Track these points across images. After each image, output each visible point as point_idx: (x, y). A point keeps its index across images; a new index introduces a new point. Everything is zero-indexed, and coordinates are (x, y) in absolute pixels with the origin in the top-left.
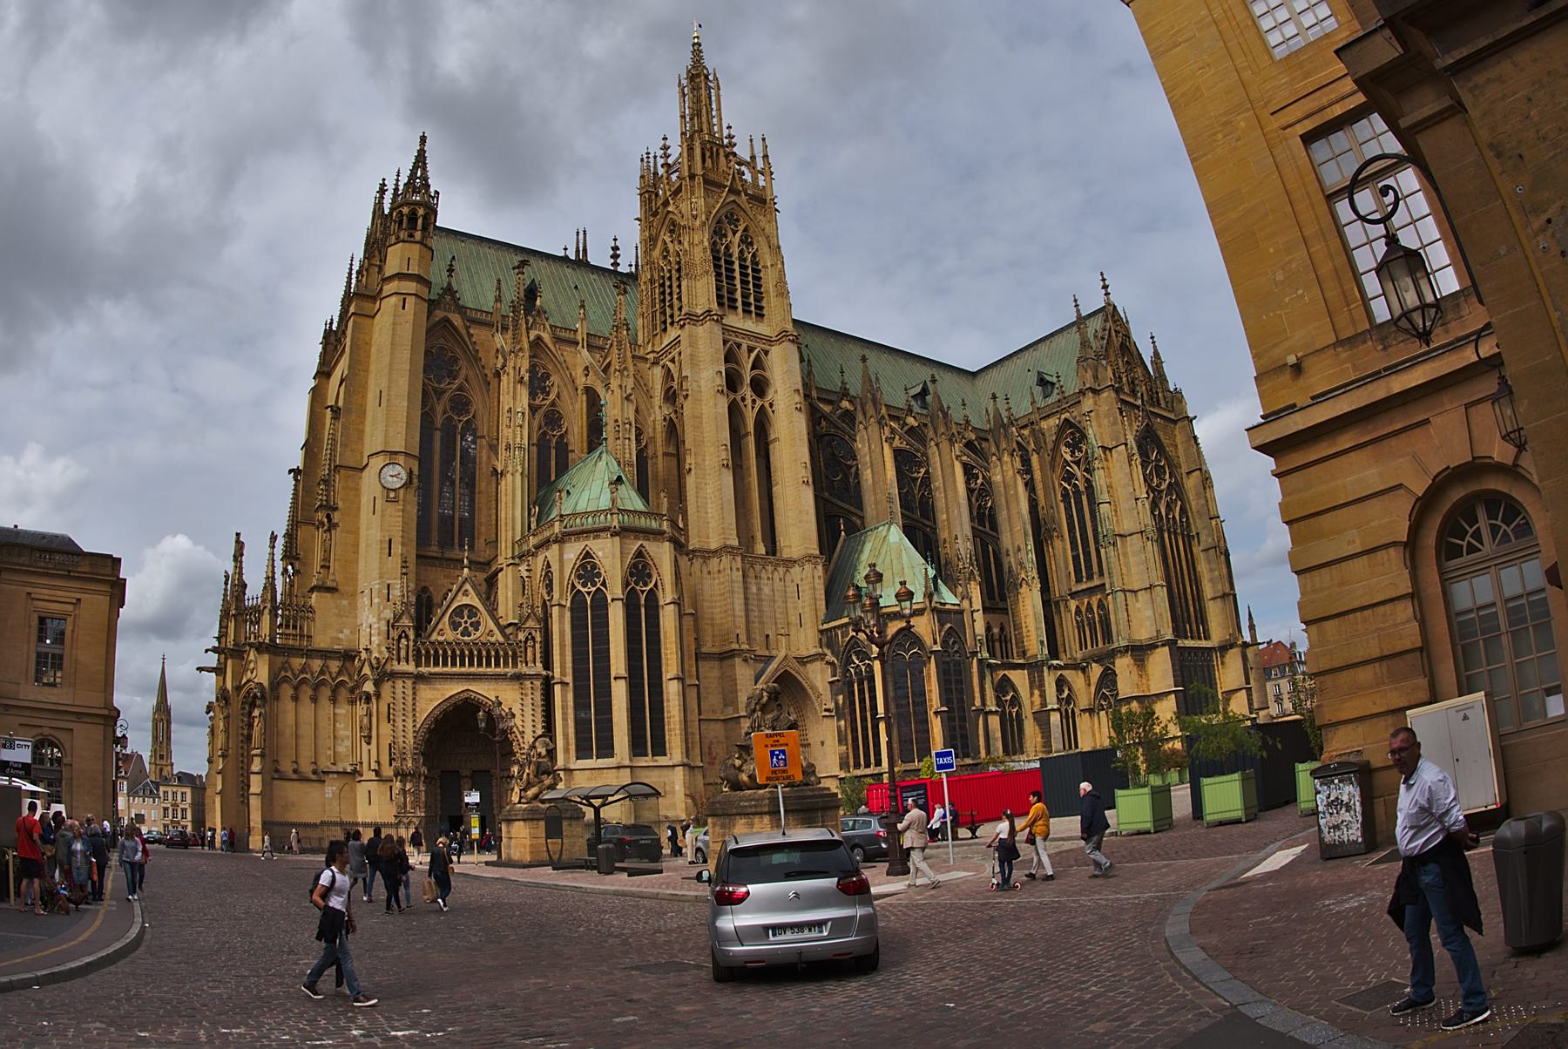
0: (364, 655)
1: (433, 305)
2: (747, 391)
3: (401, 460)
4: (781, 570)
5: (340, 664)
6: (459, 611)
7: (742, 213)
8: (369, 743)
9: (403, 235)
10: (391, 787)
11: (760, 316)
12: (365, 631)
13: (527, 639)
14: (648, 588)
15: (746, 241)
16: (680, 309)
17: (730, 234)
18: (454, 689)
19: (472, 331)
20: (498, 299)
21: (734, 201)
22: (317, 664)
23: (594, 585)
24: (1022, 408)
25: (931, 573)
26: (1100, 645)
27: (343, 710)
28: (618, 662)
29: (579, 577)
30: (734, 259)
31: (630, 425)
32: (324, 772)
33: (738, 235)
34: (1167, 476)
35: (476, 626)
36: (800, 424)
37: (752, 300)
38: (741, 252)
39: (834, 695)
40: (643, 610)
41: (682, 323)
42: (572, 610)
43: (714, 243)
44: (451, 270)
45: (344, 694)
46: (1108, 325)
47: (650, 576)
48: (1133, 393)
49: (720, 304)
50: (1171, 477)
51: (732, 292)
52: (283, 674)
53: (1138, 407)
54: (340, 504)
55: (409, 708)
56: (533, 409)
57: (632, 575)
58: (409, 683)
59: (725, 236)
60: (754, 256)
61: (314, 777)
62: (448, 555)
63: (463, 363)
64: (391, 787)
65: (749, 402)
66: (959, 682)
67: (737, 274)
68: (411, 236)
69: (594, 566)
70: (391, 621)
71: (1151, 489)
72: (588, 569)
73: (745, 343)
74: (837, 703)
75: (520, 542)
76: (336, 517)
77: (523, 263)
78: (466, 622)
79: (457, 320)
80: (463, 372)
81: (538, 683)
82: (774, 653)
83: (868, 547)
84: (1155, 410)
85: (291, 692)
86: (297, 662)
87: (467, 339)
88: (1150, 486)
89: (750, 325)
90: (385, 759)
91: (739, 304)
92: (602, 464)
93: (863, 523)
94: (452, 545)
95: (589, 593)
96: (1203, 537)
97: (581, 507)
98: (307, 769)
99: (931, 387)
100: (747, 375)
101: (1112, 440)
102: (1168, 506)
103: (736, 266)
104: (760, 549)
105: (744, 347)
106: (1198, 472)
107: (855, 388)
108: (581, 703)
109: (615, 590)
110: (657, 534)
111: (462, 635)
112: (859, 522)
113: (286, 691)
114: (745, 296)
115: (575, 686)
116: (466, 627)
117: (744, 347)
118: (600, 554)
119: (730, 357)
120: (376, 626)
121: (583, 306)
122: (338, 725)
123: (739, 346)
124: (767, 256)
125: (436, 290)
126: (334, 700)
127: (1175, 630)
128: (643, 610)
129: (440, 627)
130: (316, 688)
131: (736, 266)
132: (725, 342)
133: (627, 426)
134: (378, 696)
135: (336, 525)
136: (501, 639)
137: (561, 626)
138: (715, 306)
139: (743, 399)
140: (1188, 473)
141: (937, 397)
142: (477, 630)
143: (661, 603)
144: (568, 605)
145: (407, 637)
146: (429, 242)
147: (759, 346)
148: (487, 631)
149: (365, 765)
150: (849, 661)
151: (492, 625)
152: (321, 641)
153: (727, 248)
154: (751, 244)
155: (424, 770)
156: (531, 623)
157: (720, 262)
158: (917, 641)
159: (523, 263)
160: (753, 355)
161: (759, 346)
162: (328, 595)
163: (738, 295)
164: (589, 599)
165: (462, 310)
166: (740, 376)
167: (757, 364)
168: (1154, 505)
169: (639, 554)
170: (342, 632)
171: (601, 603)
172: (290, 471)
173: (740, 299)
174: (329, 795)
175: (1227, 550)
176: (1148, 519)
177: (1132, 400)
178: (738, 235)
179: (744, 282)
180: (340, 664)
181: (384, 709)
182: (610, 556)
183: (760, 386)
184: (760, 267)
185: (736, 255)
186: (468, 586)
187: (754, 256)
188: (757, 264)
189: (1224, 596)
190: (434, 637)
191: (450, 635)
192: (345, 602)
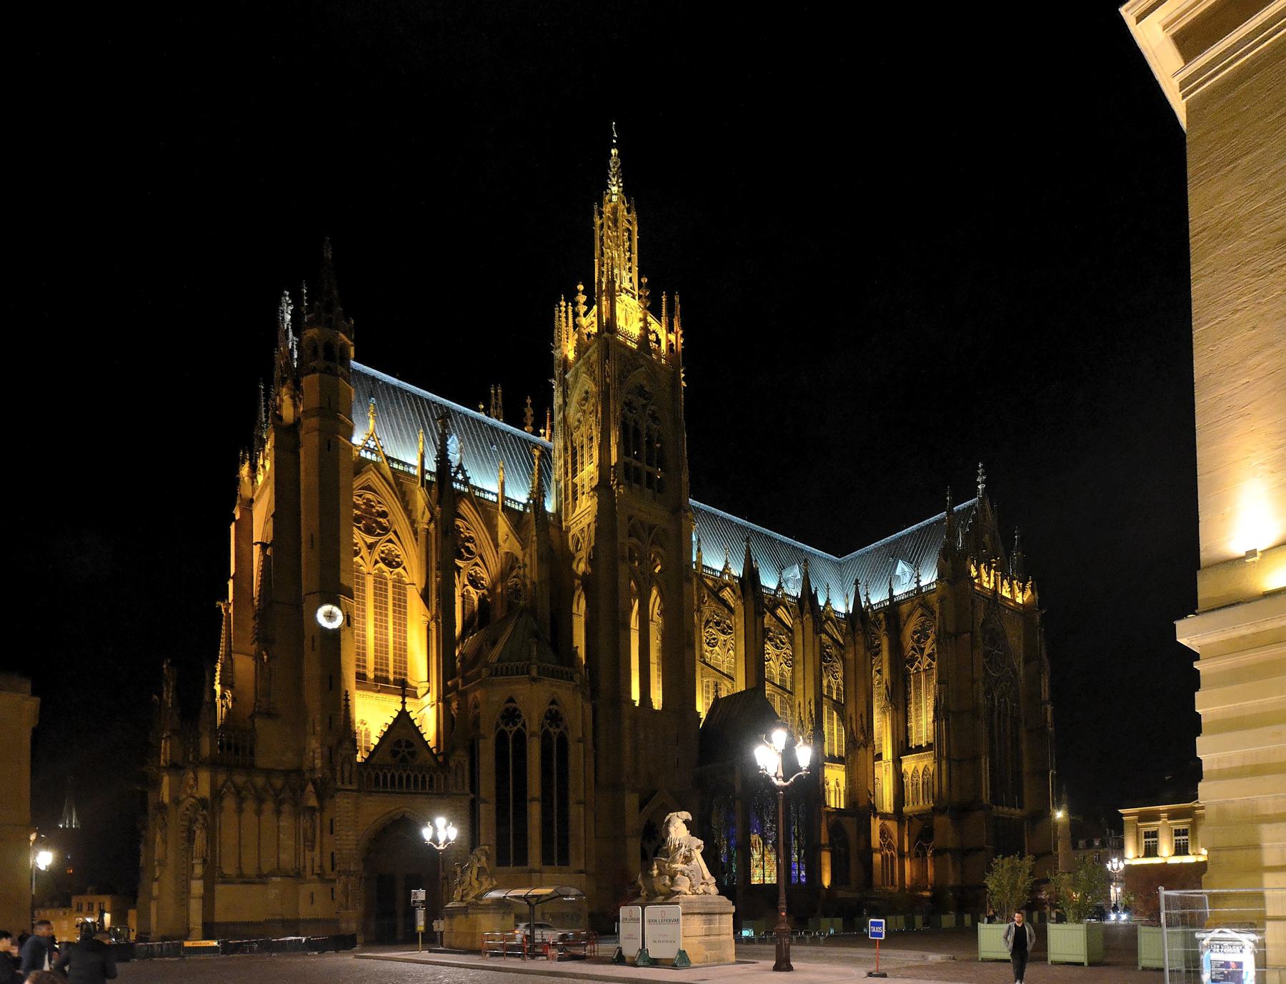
8: (313, 848)
10: (332, 889)
13: (457, 766)
57: (546, 717)
61: (258, 880)
64: (332, 889)
78: (403, 751)
90: (327, 865)
95: (511, 732)
98: (249, 870)
116: (403, 756)
120: (319, 750)
126: (278, 812)
130: (260, 801)
149: (308, 869)
164: (511, 737)
169: (553, 702)
171: (520, 739)
181: (327, 822)
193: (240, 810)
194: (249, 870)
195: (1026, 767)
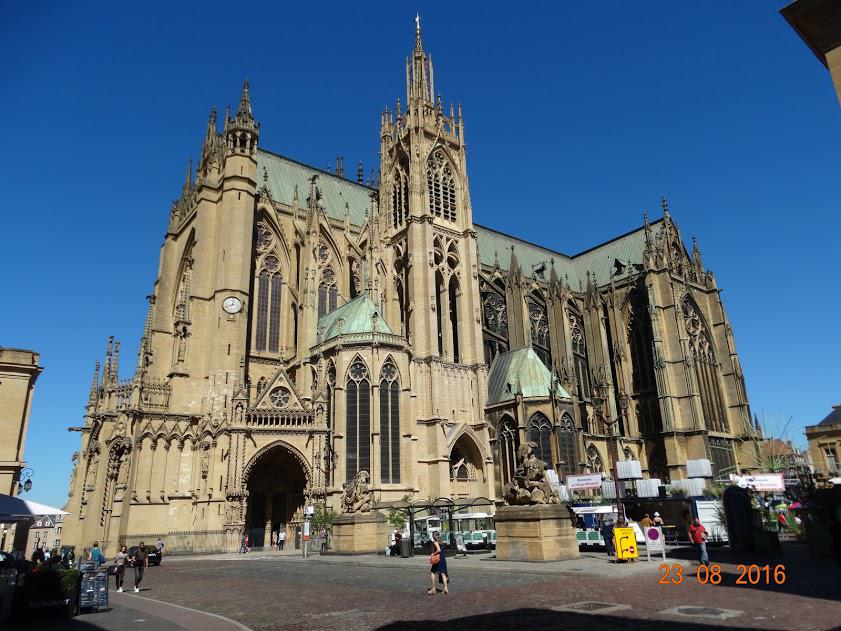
0: (207, 418)
1: (257, 198)
2: (444, 264)
3: (238, 295)
4: (462, 371)
5: (187, 423)
6: (276, 390)
9: (238, 150)
11: (454, 220)
12: (209, 402)
14: (392, 380)
15: (447, 171)
16: (407, 213)
18: (271, 439)
19: (280, 217)
20: (296, 198)
21: (440, 147)
22: (170, 424)
23: (361, 376)
24: (604, 278)
25: (555, 378)
26: (653, 429)
27: (187, 452)
28: (375, 425)
29: (352, 372)
32: (170, 498)
33: (443, 168)
34: (700, 327)
35: (286, 400)
36: (475, 284)
37: (449, 209)
39: (493, 450)
40: (390, 394)
42: (347, 391)
43: (429, 173)
44: (266, 177)
45: (188, 443)
46: (665, 230)
47: (394, 372)
48: (680, 273)
49: (432, 211)
50: (703, 326)
51: (438, 203)
52: (146, 431)
53: (682, 283)
54: (193, 321)
55: (240, 452)
56: (320, 268)
57: (384, 371)
58: (242, 436)
59: (435, 168)
60: (452, 181)
62: (262, 355)
63: (273, 237)
65: (446, 271)
66: (571, 446)
67: (441, 193)
68: (243, 151)
69: (362, 365)
70: (231, 395)
71: (690, 335)
72: (358, 366)
73: (445, 236)
74: (494, 456)
75: (312, 349)
76: (189, 329)
77: (315, 177)
79: (270, 210)
80: (273, 243)
81: (324, 437)
82: (458, 422)
83: (514, 361)
84: (694, 285)
85: (151, 443)
86: (156, 423)
87: (276, 221)
88: (688, 332)
89: (447, 224)
91: (442, 212)
92: (365, 305)
93: (508, 347)
94: (265, 348)
96: (724, 366)
97: (354, 329)
98: (156, 497)
99: (549, 267)
100: (446, 255)
101: (664, 302)
102: (700, 345)
103: (441, 188)
104: (450, 358)
105: (444, 238)
106: (722, 326)
107: (505, 265)
108: (351, 449)
109: (376, 380)
110: (399, 348)
111: (277, 405)
112: (505, 345)
113: (147, 442)
114: (446, 206)
115: (348, 439)
117: (444, 238)
118: (365, 358)
119: (437, 243)
121: (347, 207)
122: (183, 465)
123: (441, 237)
125: (258, 188)
127: (707, 425)
128: (390, 394)
129: (262, 400)
131: (441, 188)
134: (215, 445)
135: (190, 334)
136: (302, 409)
137: (341, 400)
138: (428, 213)
139: (443, 269)
140: (714, 326)
141: (553, 272)
142: (286, 402)
143: (401, 389)
144: (345, 388)
145: (242, 406)
146: (254, 157)
147: (453, 238)
148: (293, 404)
150: (503, 429)
151: (296, 400)
152: (175, 409)
153: (436, 176)
154: (449, 174)
155: (247, 492)
156: (320, 399)
157: (433, 185)
158: (546, 419)
159: (315, 177)
160: (449, 243)
161: (453, 238)
162: (183, 379)
163: (441, 206)
165: (273, 203)
166: (442, 256)
167: (452, 248)
168: (691, 344)
169: (389, 359)
170: (190, 403)
171: (366, 388)
172: (148, 297)
173: (442, 209)
174: (171, 513)
175: (742, 376)
176: (689, 354)
177: (677, 278)
178: (443, 168)
180: (187, 423)
182: (375, 361)
183: (452, 263)
185: (441, 181)
186: (282, 375)
187: (452, 181)
189: (741, 406)
190: (259, 407)
191: (270, 405)
192: (194, 384)
193: (154, 448)
194: (156, 497)
195: (727, 402)
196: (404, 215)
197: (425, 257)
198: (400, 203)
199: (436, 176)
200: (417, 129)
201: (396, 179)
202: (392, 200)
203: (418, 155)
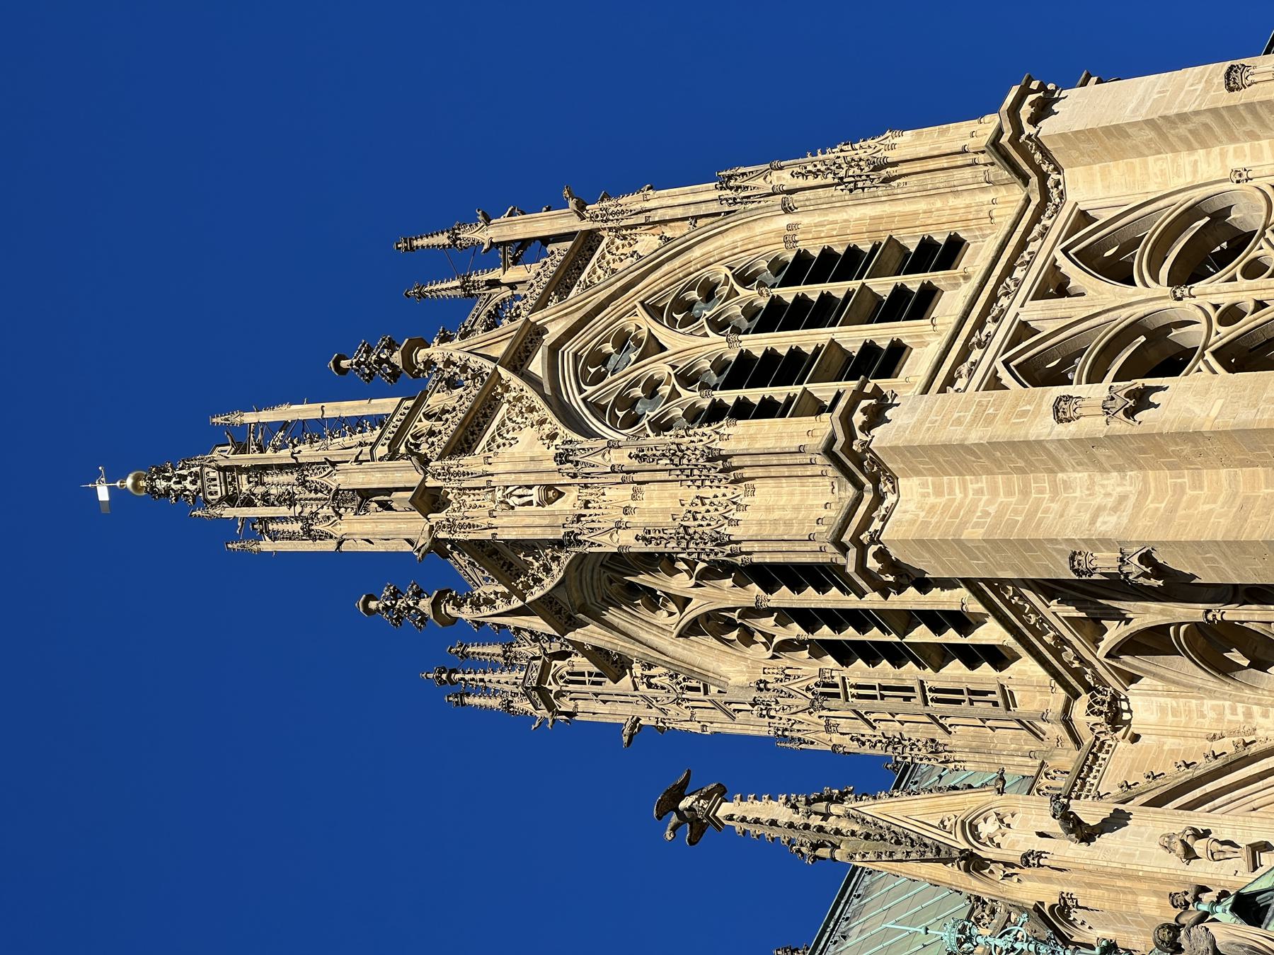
7: (600, 321)
11: (954, 247)
17: (659, 368)
30: (732, 356)
31: (1198, 835)
33: (663, 334)
38: (718, 325)
41: (872, 564)
60: (745, 278)
65: (1243, 292)
123: (1024, 330)
124: (759, 228)
132: (994, 383)
133: (1199, 846)
139: (1231, 314)
153: (688, 378)
160: (1077, 276)
178: (663, 334)
179: (823, 313)
184: (790, 256)
187: (745, 278)
188: (776, 265)
196: (834, 599)
197: (1087, 449)
198: (861, 619)
199: (688, 378)
200: (429, 500)
201: (748, 637)
202: (859, 671)
203: (552, 493)
